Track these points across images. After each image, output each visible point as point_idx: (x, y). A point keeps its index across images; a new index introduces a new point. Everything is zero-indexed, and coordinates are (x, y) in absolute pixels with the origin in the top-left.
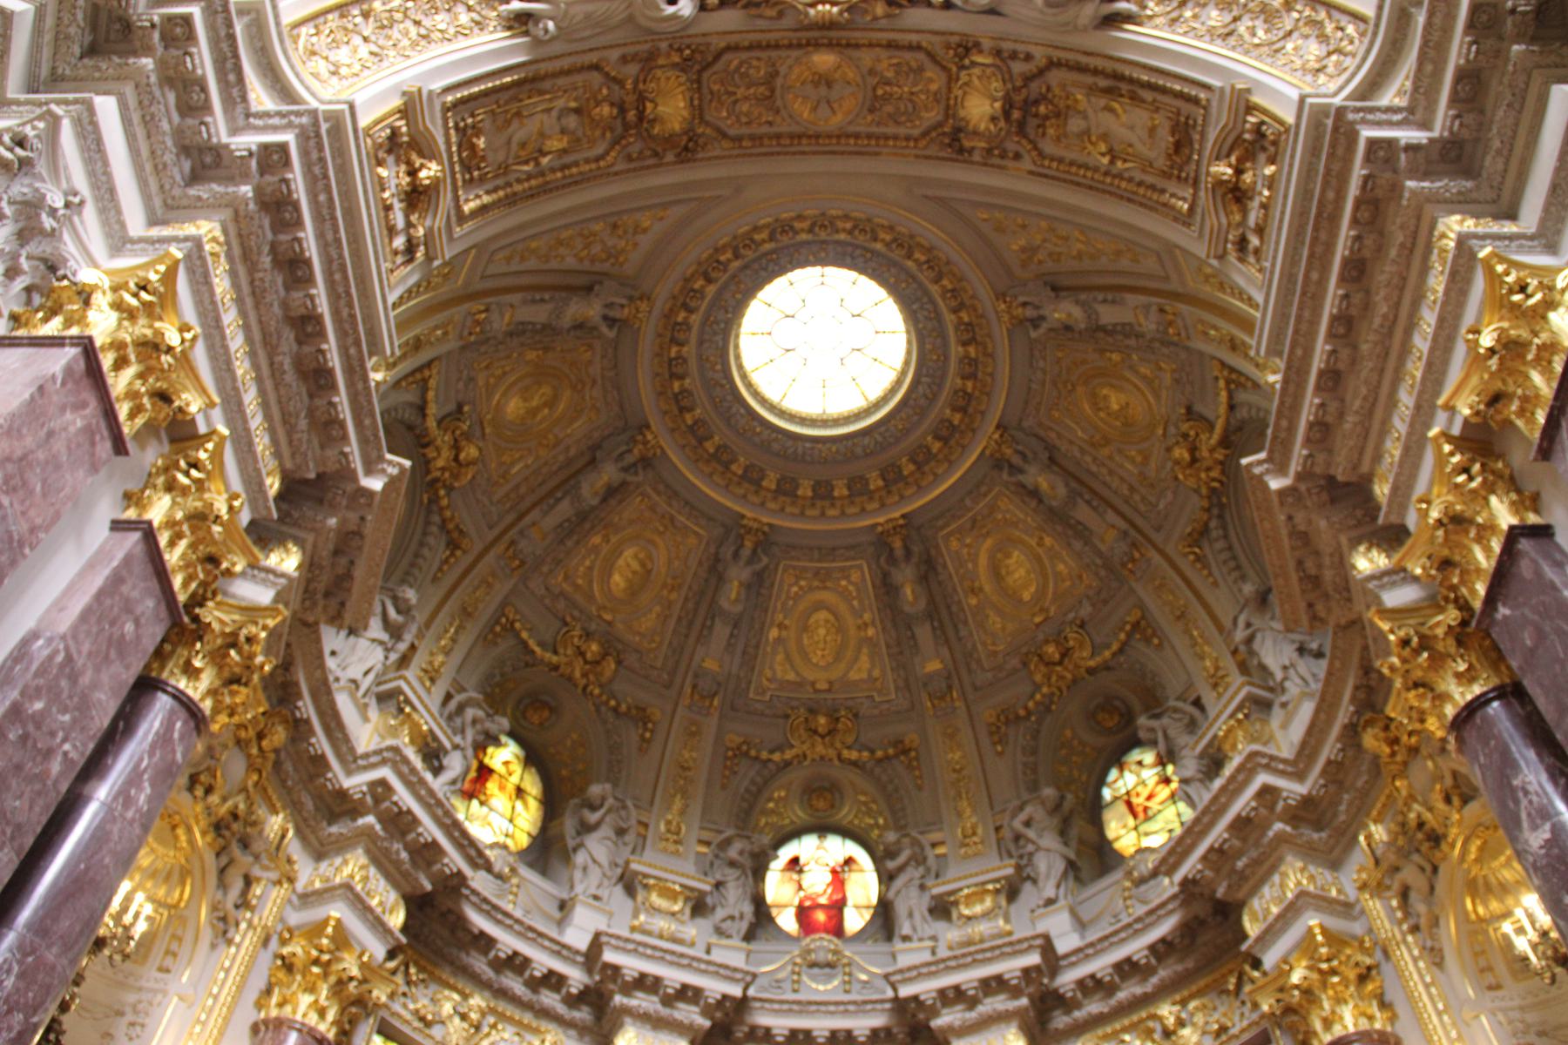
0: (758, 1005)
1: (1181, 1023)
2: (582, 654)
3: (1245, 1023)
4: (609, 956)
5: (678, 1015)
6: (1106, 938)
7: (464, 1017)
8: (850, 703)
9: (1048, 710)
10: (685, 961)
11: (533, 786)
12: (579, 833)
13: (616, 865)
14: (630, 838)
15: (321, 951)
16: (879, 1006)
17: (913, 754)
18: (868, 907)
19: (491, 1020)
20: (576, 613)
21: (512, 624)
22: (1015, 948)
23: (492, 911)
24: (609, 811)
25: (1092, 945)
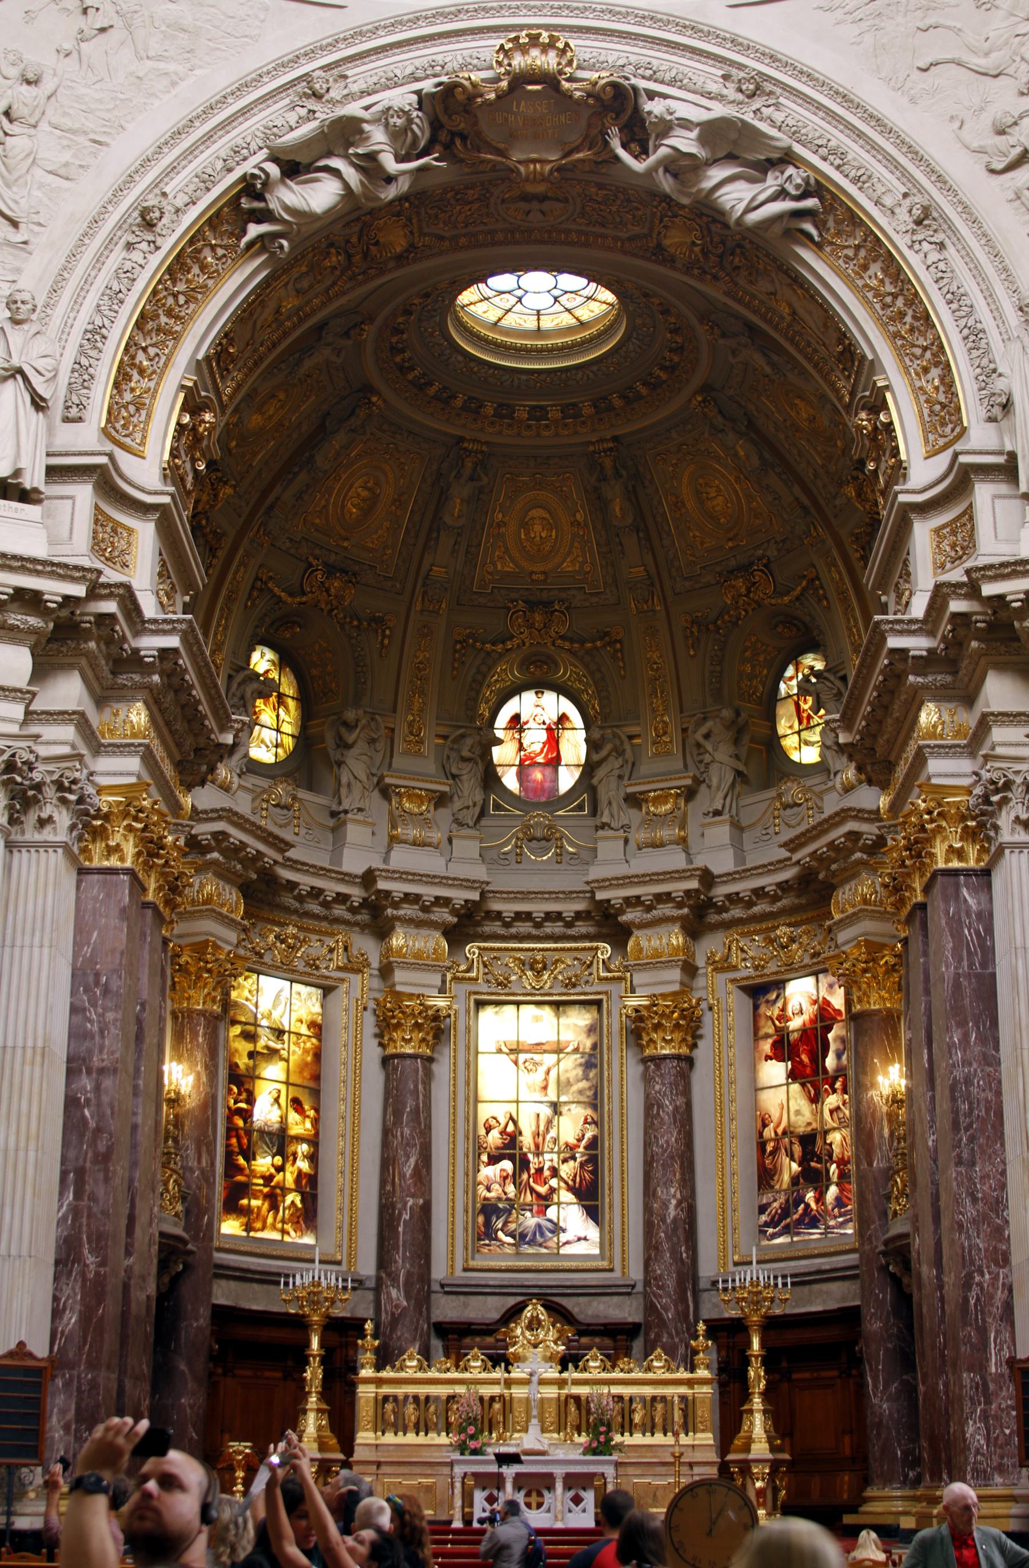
2: (327, 590)
4: (382, 885)
5: (433, 917)
6: (748, 870)
7: (282, 942)
8: (564, 595)
9: (735, 624)
11: (288, 688)
12: (338, 746)
13: (373, 775)
14: (380, 745)
15: (207, 962)
17: (618, 646)
18: (578, 766)
20: (317, 552)
21: (266, 583)
23: (294, 865)
24: (363, 728)
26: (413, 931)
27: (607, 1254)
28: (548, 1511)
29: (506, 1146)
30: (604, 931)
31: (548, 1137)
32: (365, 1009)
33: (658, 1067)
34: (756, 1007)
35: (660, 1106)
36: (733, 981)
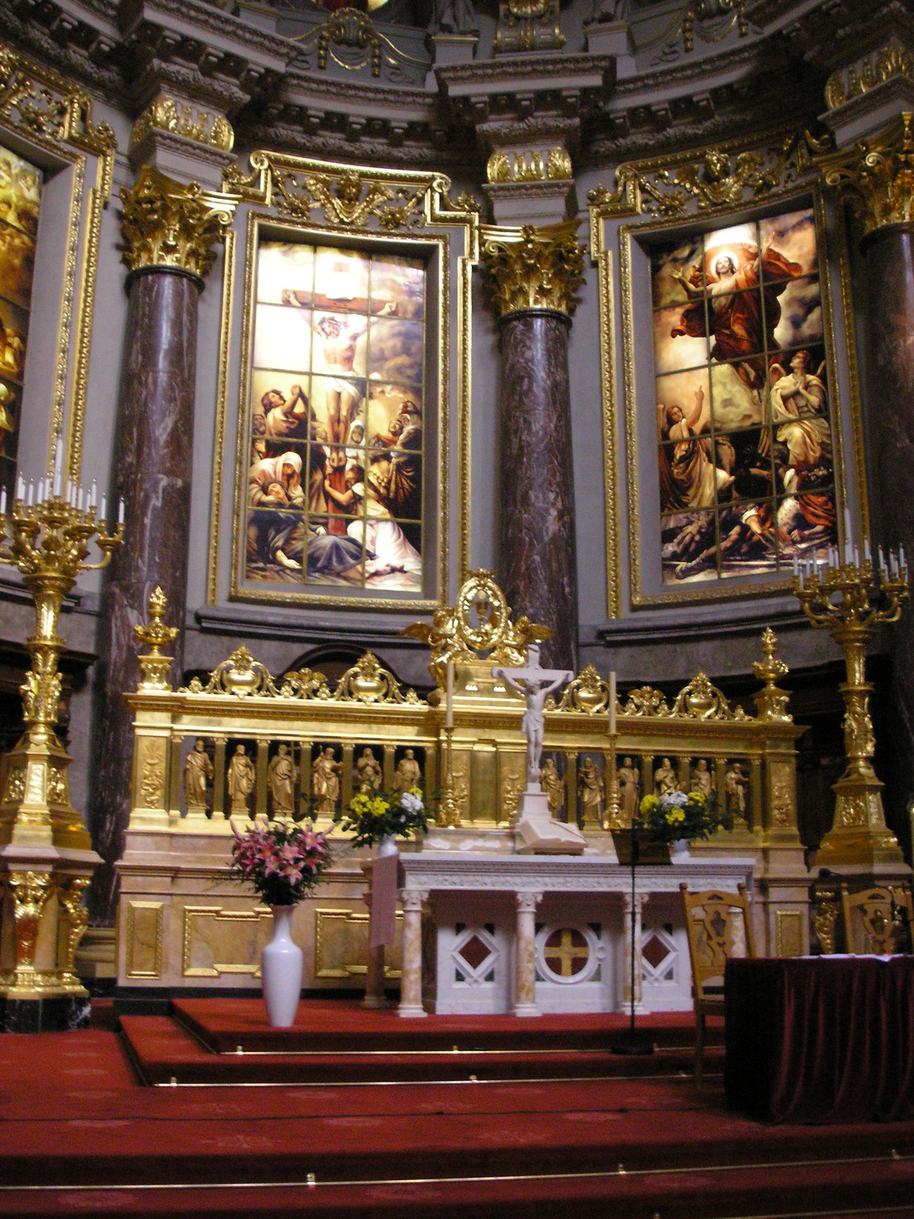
0: (295, 82)
1: (725, 172)
3: (790, 185)
5: (217, 87)
10: (230, 28)
16: (420, 100)
19: (21, 75)
22: (577, 66)
25: (654, 76)
26: (187, 104)
27: (440, 589)
28: (597, 977)
29: (291, 433)
30: (444, 155)
31: (353, 426)
32: (106, 205)
33: (529, 327)
34: (656, 269)
35: (531, 378)
36: (629, 228)
